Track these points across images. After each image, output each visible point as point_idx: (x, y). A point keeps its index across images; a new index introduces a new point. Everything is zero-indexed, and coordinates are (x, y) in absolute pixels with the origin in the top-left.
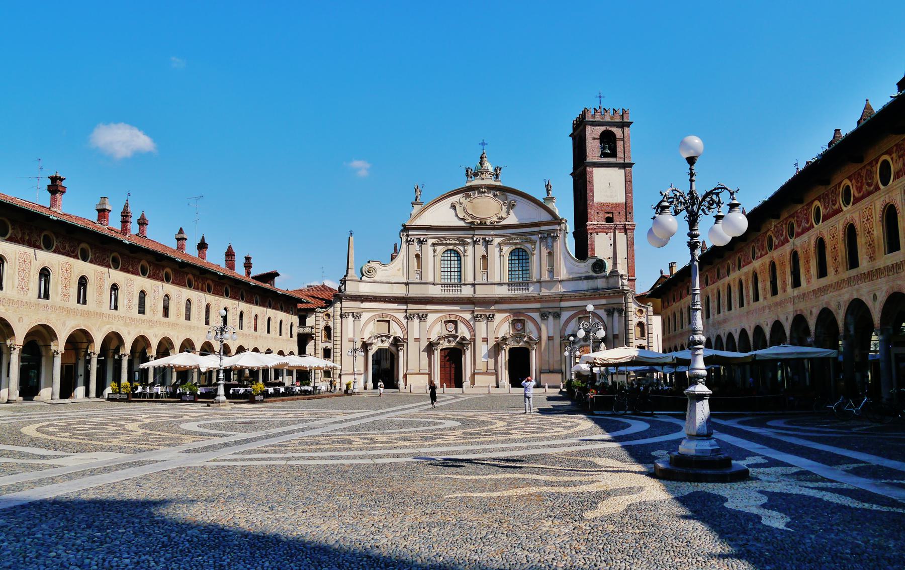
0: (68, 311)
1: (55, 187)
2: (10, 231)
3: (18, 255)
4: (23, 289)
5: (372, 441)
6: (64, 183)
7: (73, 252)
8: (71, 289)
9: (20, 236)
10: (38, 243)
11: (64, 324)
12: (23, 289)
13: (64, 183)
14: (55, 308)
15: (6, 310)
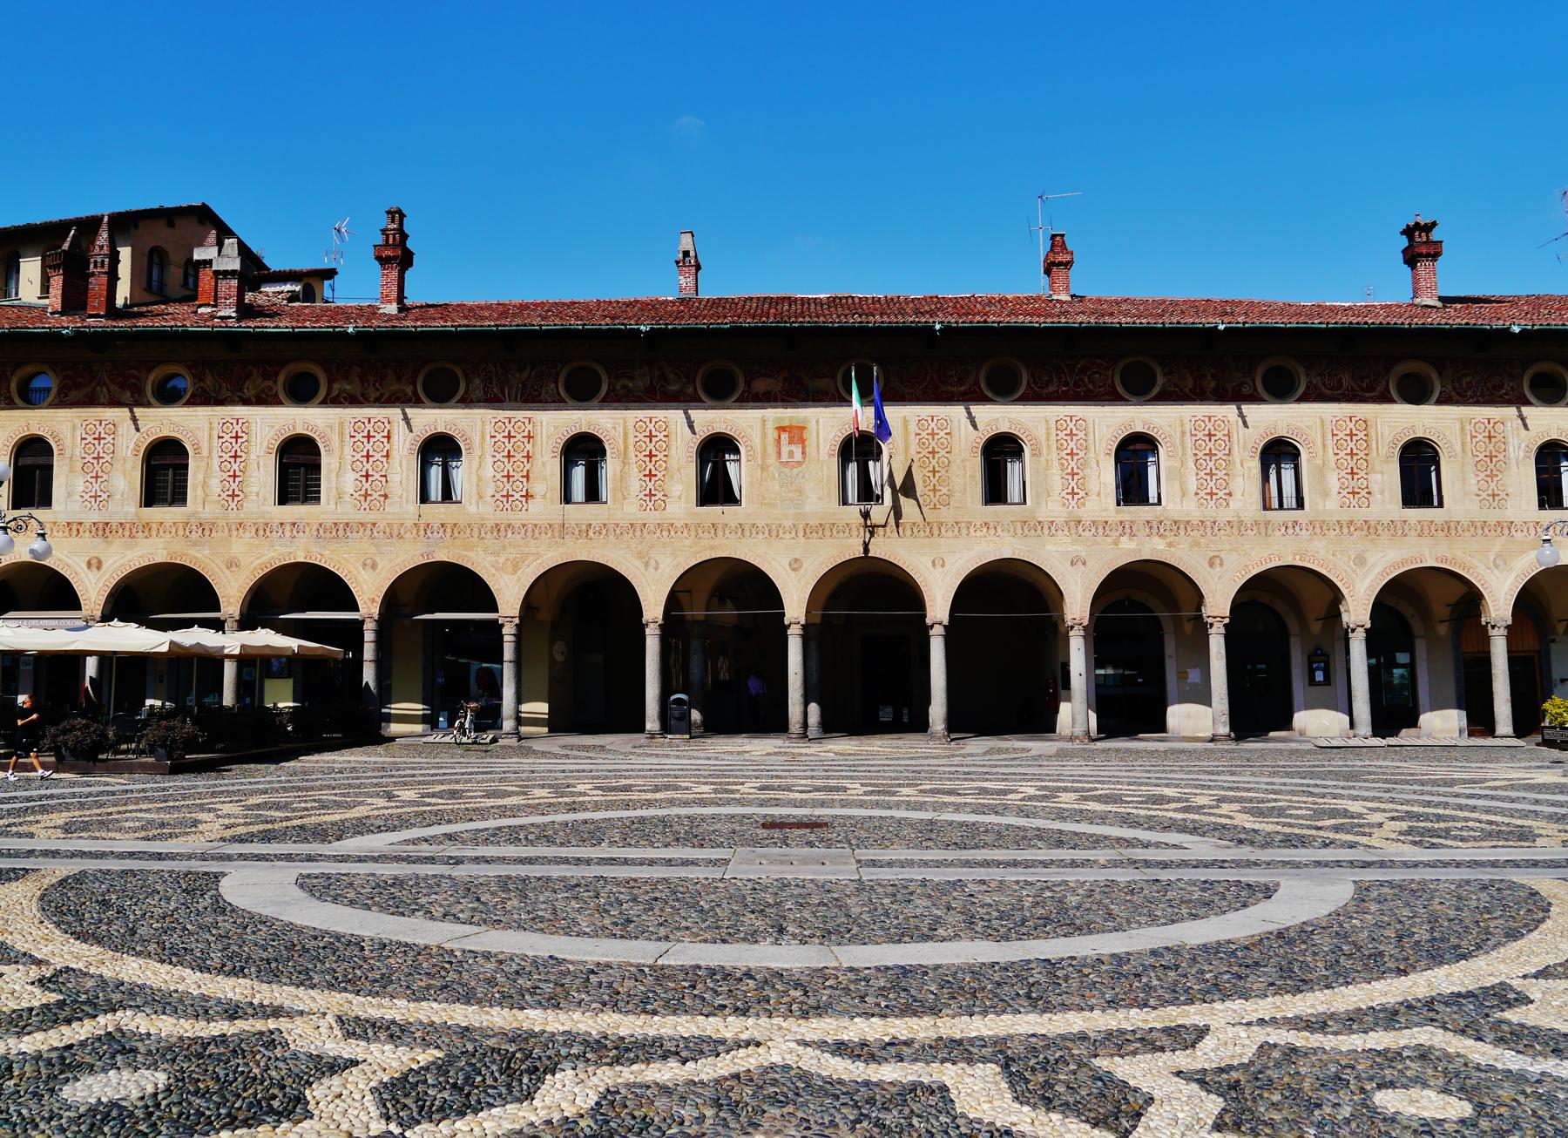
0: (1370, 529)
1: (1420, 246)
2: (1160, 381)
3: (1188, 427)
4: (1357, 495)
5: (559, 790)
6: (1435, 235)
7: (1371, 388)
8: (1375, 478)
9: (1190, 383)
10: (1246, 390)
11: (1360, 561)
12: (1357, 495)
13: (1435, 235)
14: (1321, 527)
15: (1170, 545)
